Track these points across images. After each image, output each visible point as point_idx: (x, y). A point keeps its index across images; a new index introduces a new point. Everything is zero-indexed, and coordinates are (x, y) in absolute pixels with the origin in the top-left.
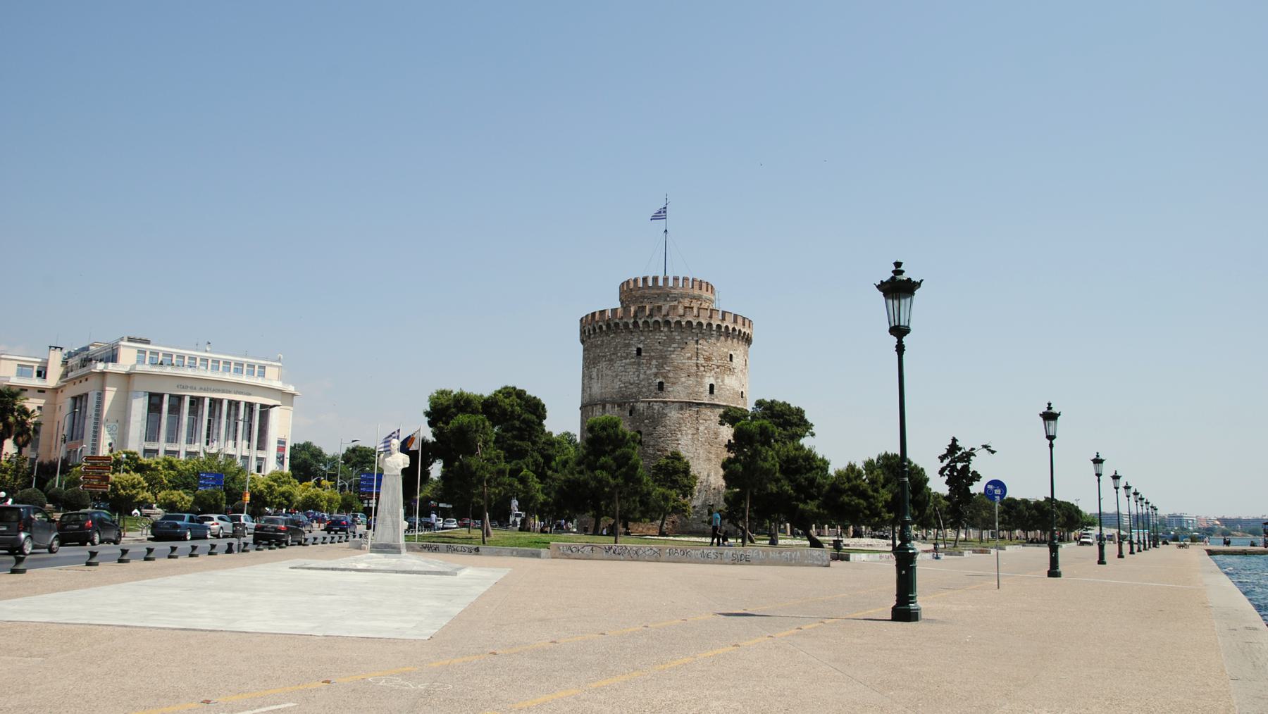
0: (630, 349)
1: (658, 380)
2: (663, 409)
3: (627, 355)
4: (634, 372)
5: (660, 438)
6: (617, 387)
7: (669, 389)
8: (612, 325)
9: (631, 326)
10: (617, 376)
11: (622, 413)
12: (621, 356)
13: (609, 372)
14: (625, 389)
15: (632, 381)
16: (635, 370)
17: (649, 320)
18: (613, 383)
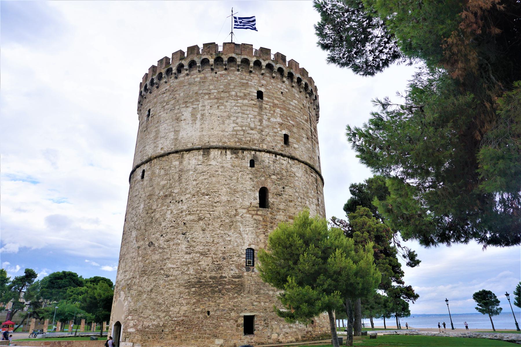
0: (249, 90)
1: (284, 132)
2: (291, 167)
3: (245, 95)
4: (256, 116)
5: (291, 201)
6: (231, 129)
7: (296, 146)
8: (225, 59)
9: (252, 64)
10: (229, 117)
11: (237, 162)
12: (236, 96)
13: (217, 112)
14: (242, 133)
15: (252, 125)
16: (256, 114)
17: (273, 64)
18: (224, 123)
